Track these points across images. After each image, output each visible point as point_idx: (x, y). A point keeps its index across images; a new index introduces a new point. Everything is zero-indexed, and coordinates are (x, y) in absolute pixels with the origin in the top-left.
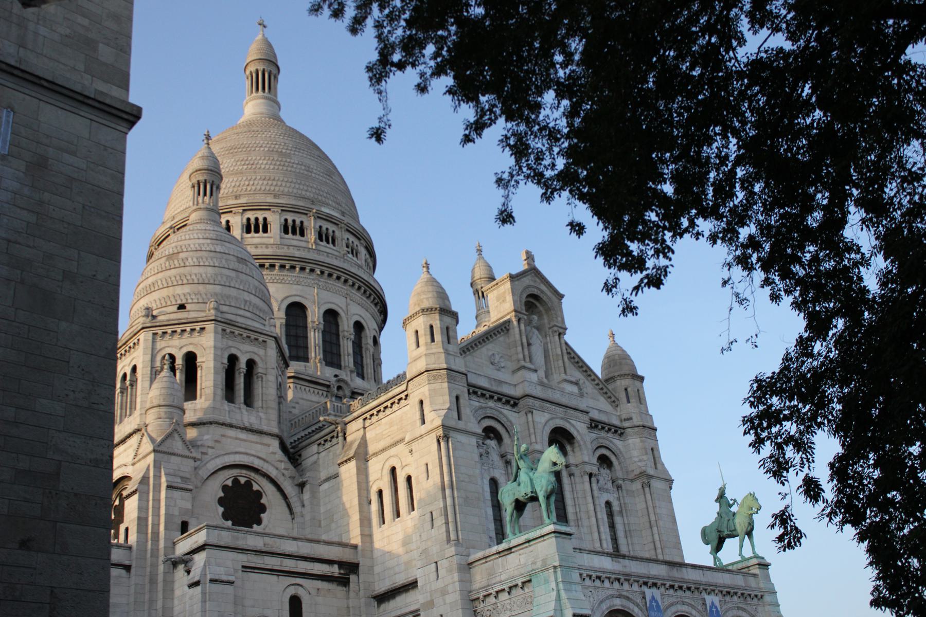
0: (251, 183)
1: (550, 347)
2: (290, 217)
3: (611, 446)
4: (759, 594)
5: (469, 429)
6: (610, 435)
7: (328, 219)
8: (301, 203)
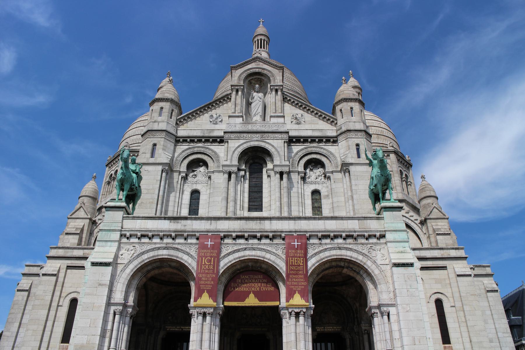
0: (226, 89)
3: (321, 151)
5: (158, 162)
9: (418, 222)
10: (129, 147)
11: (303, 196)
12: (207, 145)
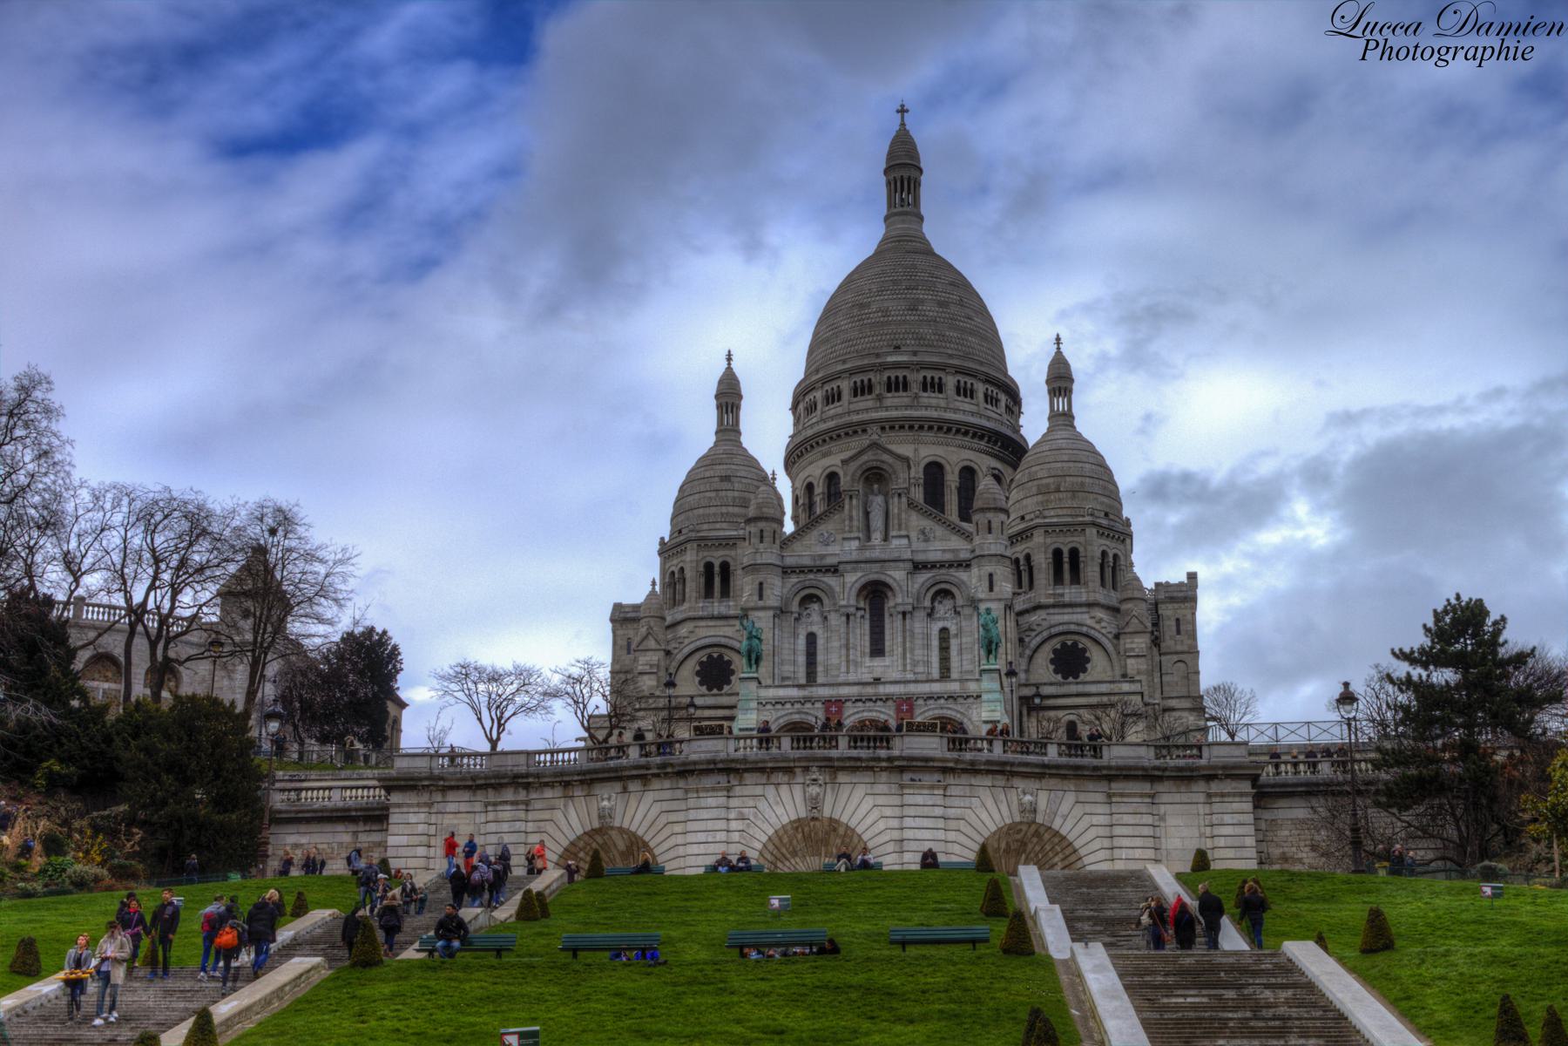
1: (891, 507)
2: (858, 378)
3: (951, 579)
4: (975, 695)
6: (952, 571)
7: (897, 366)
8: (866, 362)
9: (1110, 636)
10: (698, 532)
11: (928, 636)
12: (819, 576)
